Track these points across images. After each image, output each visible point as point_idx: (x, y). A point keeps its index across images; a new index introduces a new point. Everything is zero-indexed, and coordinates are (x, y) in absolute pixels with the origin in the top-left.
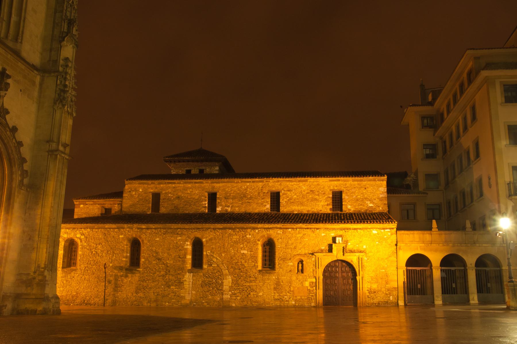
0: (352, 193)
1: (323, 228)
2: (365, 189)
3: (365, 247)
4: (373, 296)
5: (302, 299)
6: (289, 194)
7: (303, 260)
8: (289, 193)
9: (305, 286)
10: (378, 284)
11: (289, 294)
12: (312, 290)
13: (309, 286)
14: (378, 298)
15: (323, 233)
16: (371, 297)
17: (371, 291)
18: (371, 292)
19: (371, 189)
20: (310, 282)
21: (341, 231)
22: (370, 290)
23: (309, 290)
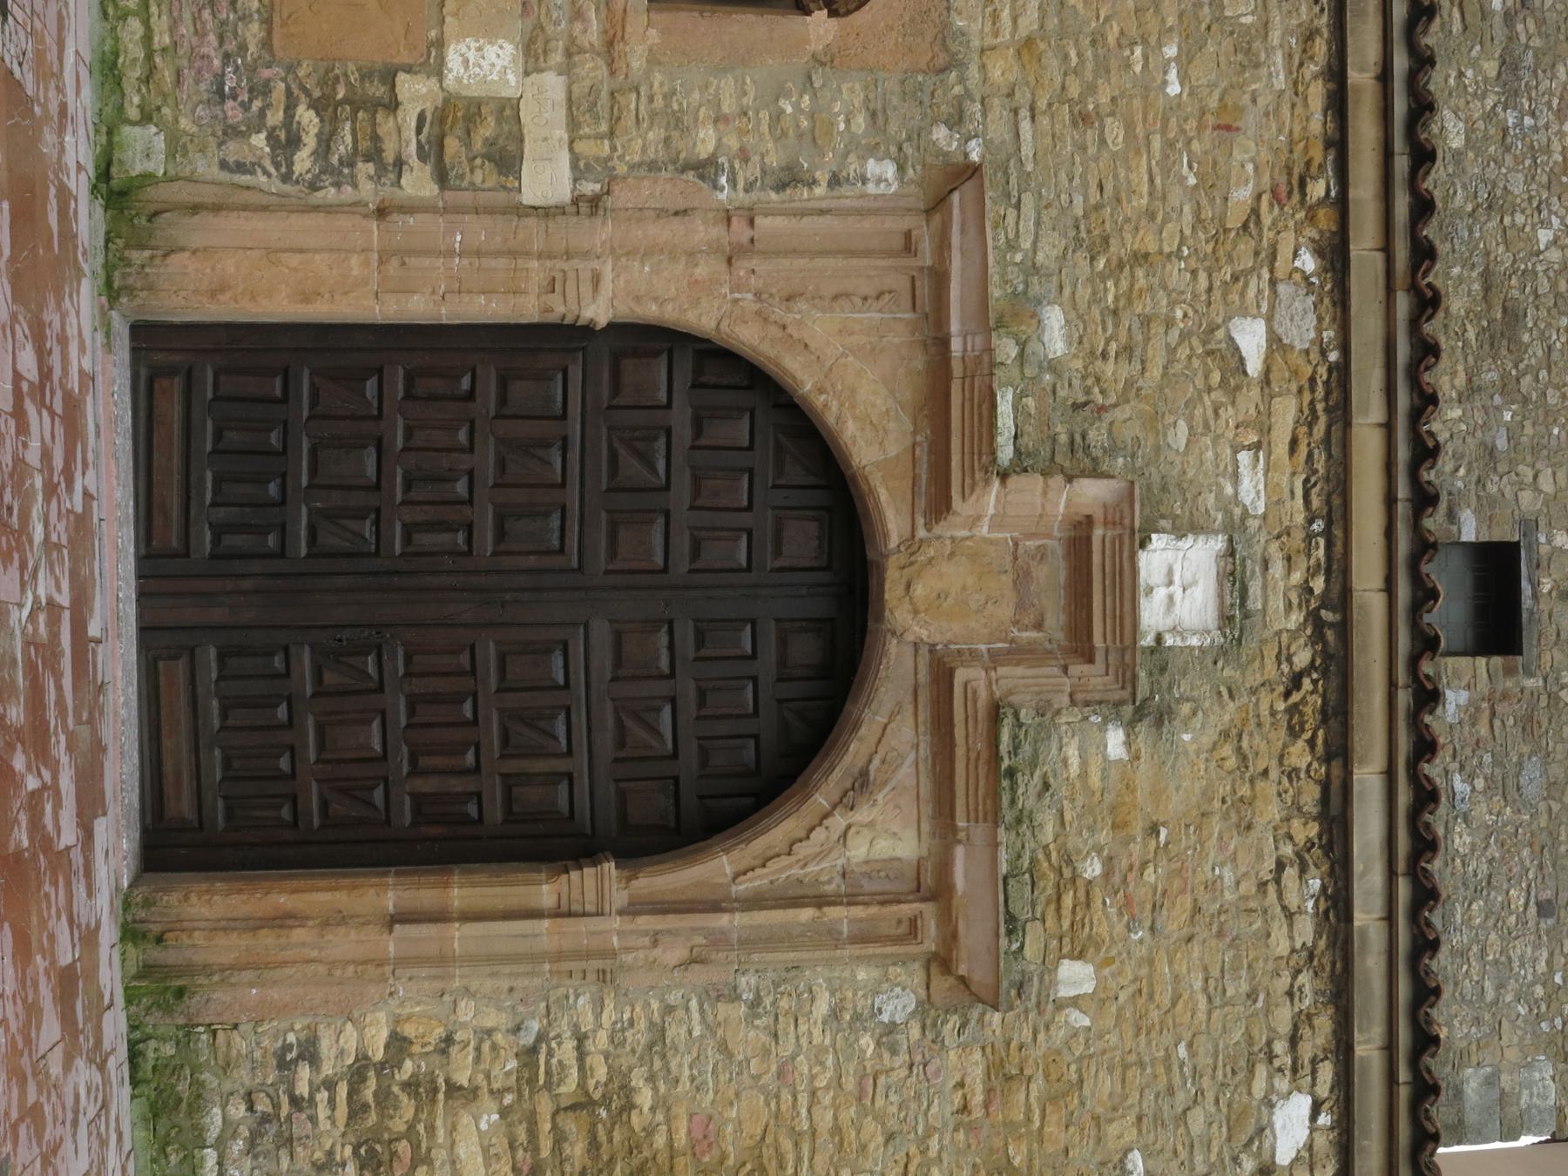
0: (1496, 763)
1: (1345, 349)
2: (1545, 909)
4: (301, 1127)
6: (1474, 64)
8: (1491, 67)
12: (376, 138)
15: (1275, 343)
16: (295, 1101)
17: (383, 1096)
18: (368, 1094)
19: (1542, 967)
20: (508, 110)
21: (1296, 618)
22: (410, 1086)
23: (377, 90)
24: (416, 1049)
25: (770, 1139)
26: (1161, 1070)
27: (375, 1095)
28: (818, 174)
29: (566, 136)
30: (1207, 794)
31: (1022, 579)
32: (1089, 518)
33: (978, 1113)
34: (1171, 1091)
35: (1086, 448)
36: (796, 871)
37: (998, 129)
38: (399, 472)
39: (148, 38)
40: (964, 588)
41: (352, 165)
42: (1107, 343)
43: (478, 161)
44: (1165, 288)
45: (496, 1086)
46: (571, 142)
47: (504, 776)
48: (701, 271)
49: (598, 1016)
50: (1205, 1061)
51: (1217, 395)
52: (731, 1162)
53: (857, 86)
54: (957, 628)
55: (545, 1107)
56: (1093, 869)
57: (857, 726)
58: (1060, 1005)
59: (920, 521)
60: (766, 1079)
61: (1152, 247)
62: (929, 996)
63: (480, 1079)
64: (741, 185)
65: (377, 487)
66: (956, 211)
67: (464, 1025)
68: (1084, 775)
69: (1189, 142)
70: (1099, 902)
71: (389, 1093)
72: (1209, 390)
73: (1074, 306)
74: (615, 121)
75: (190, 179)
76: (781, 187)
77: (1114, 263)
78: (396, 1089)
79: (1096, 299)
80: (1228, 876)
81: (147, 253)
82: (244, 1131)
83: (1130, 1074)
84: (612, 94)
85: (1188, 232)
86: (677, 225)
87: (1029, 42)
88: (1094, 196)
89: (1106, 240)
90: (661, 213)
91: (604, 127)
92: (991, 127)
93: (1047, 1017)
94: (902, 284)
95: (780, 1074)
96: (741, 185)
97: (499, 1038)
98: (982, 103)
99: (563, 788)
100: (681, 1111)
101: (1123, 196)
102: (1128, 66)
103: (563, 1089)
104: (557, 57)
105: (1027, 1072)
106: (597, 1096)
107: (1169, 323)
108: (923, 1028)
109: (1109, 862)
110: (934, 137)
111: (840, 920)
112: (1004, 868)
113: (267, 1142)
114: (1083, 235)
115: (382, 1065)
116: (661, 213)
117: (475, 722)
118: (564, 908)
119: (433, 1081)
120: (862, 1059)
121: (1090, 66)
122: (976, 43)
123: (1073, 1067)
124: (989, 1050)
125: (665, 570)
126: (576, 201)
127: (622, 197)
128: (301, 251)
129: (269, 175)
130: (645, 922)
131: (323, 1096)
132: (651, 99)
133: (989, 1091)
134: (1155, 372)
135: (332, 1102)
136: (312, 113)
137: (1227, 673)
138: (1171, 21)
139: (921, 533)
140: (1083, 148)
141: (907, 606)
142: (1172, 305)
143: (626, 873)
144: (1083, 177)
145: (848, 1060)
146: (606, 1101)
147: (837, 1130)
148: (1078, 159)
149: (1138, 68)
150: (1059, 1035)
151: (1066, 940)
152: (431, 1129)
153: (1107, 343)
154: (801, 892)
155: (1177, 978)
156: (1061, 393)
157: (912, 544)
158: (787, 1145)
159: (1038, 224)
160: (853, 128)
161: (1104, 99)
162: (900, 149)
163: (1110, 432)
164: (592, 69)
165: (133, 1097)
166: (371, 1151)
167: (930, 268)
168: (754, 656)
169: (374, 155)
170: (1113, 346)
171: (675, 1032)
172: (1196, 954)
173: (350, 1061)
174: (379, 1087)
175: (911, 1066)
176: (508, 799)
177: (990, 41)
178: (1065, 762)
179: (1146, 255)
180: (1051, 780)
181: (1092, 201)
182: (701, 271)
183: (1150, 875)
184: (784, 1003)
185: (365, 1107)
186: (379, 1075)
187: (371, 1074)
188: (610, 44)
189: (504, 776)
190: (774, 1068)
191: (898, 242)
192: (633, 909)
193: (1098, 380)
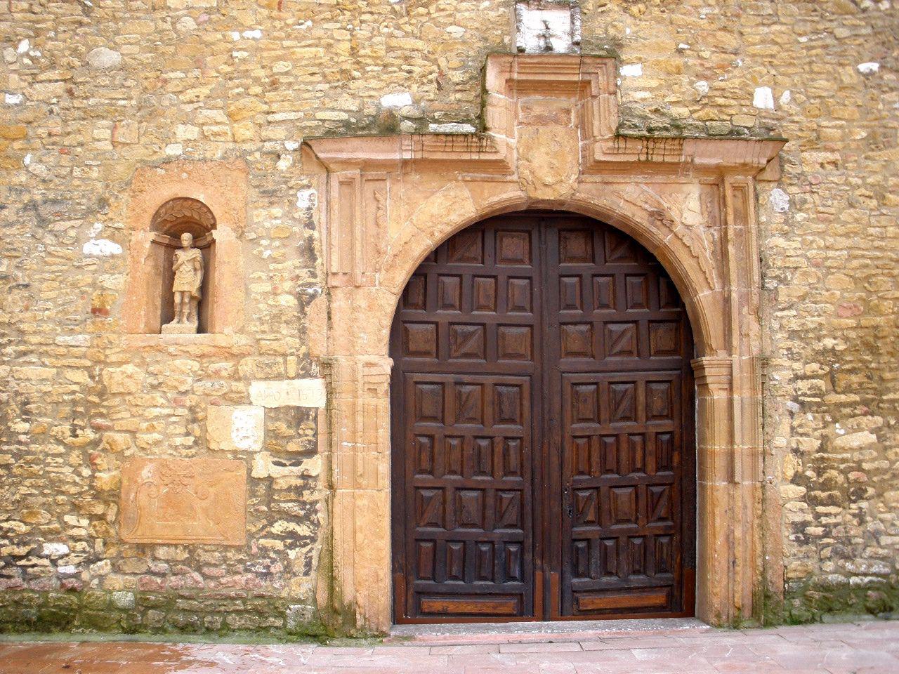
3: (763, 98)
5: (199, 569)
7: (217, 212)
9: (223, 446)
10: (879, 420)
11: (85, 522)
12: (289, 489)
13: (257, 447)
14: (885, 540)
17: (825, 486)
22: (819, 472)
23: (262, 489)
24: (800, 469)
25: (852, 273)
26: (814, 52)
27: (823, 491)
28: (306, 235)
29: (286, 381)
30: (659, 21)
31: (542, 121)
32: (507, 81)
33: (837, 156)
34: (825, 47)
35: (464, 83)
36: (708, 254)
37: (280, 133)
38: (475, 478)
39: (238, 612)
40: (547, 154)
41: (304, 503)
42: (403, 71)
43: (301, 432)
44: (370, 38)
45: (821, 425)
46: (289, 378)
47: (647, 419)
48: (363, 303)
49: (785, 368)
50: (809, 27)
51: (432, 9)
52: (863, 294)
53: (256, 212)
54: (570, 158)
55: (833, 398)
56: (703, 86)
57: (625, 217)
58: (778, 107)
59: (509, 178)
60: (819, 274)
61: (347, 45)
62: (775, 181)
63: (817, 434)
64: (313, 280)
65: (483, 490)
66: (329, 155)
67: (789, 443)
68: (651, 90)
69: (288, 25)
70: (722, 84)
71: (823, 484)
72: (429, 13)
73: (381, 89)
74: (276, 353)
75: (315, 593)
76: (313, 258)
77: (356, 66)
78: (821, 480)
79: (377, 78)
80: (705, 11)
81: (358, 616)
82: (841, 562)
83: (816, 69)
84: (261, 354)
85: (339, 25)
86: (335, 318)
87: (229, 116)
88: (318, 78)
89: (342, 71)
90: (330, 327)
91: (280, 360)
92: (278, 136)
93: (785, 115)
94: (369, 187)
95: (817, 266)
96: (313, 280)
97: (795, 423)
98: (265, 141)
99: (654, 386)
100: (836, 321)
101: (317, 62)
102: (244, 60)
103: (824, 389)
104: (240, 386)
105: (815, 126)
106: (827, 369)
107: (391, 36)
108: (791, 185)
109: (699, 76)
110: (285, 169)
111: (735, 229)
112: (703, 135)
113: (848, 550)
114: (340, 84)
115: (810, 489)
116: (330, 327)
117: (616, 436)
118: (726, 386)
119: (817, 459)
120: (808, 220)
121: (243, 81)
122: (231, 145)
123: (812, 101)
124: (803, 148)
125: (531, 326)
126: (324, 377)
127: (320, 350)
128: (355, 532)
129: (312, 549)
130: (735, 342)
131: (824, 520)
132: (264, 332)
133: (826, 149)
134: (420, 44)
135: (826, 515)
136: (276, 525)
137: (591, 8)
138: (219, 36)
139: (515, 177)
140: (290, 84)
141: (557, 187)
142: (380, 34)
143: (708, 351)
144: (306, 84)
145: (809, 228)
146: (831, 364)
147: (847, 235)
148: (296, 87)
149: (245, 54)
150: (795, 109)
151: (743, 102)
152: (843, 461)
153: (403, 71)
154: (719, 251)
155: (763, 42)
156: (432, 96)
157: (521, 183)
158: (855, 263)
159: (333, 109)
160: (279, 215)
161: (261, 73)
162: (291, 188)
163: (455, 69)
164: (247, 366)
165: (821, 622)
166: (853, 494)
167: (362, 170)
168: (579, 276)
169: (298, 490)
170: (405, 67)
171: (794, 325)
172: (749, 30)
173: (805, 505)
174: (820, 490)
175: (813, 192)
176: (660, 417)
177: (229, 138)
178: (643, 100)
179: (352, 49)
180: (654, 108)
181: (321, 79)
182: (363, 303)
183: (706, 54)
184: (779, 263)
185: (830, 497)
186: (813, 489)
187: (812, 493)
188: (233, 355)
189: (647, 419)
190: (814, 269)
191: (346, 190)
192: (728, 347)
193: (424, 76)
